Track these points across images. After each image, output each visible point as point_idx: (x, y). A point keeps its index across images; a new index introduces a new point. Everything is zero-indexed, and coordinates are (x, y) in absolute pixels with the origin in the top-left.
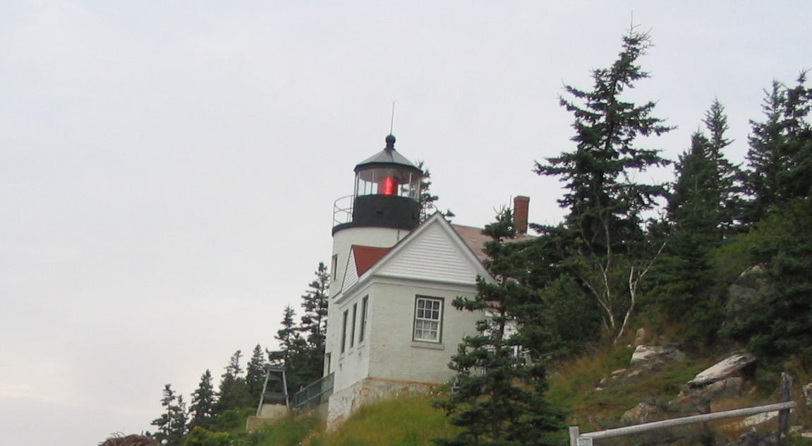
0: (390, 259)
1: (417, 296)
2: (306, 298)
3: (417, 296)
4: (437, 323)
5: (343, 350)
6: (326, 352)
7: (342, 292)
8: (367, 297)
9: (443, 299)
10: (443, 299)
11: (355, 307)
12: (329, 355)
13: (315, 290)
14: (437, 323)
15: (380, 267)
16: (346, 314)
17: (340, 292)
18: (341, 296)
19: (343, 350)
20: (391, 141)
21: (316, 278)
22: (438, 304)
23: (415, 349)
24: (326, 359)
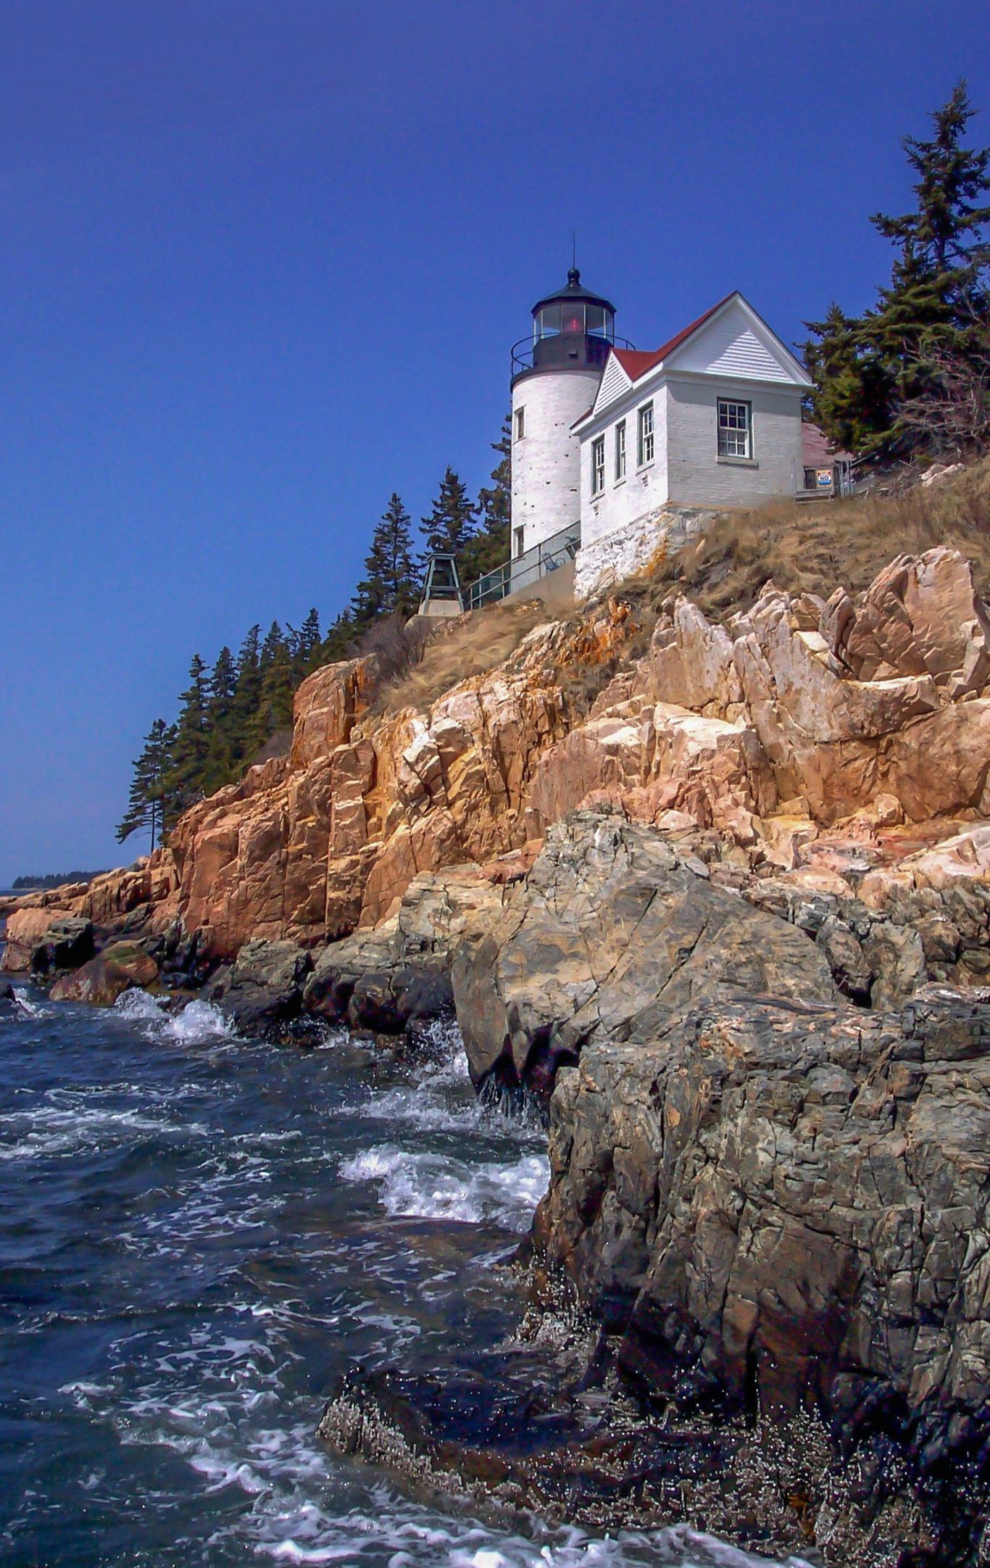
0: (699, 336)
1: (719, 399)
2: (380, 531)
3: (719, 399)
4: (743, 434)
5: (597, 484)
6: (514, 527)
7: (595, 413)
8: (651, 404)
9: (749, 403)
10: (749, 403)
11: (621, 427)
12: (520, 532)
13: (388, 523)
14: (743, 434)
15: (675, 360)
16: (599, 444)
17: (590, 413)
18: (591, 418)
19: (597, 484)
20: (574, 276)
21: (388, 509)
22: (743, 408)
23: (723, 467)
24: (514, 539)
